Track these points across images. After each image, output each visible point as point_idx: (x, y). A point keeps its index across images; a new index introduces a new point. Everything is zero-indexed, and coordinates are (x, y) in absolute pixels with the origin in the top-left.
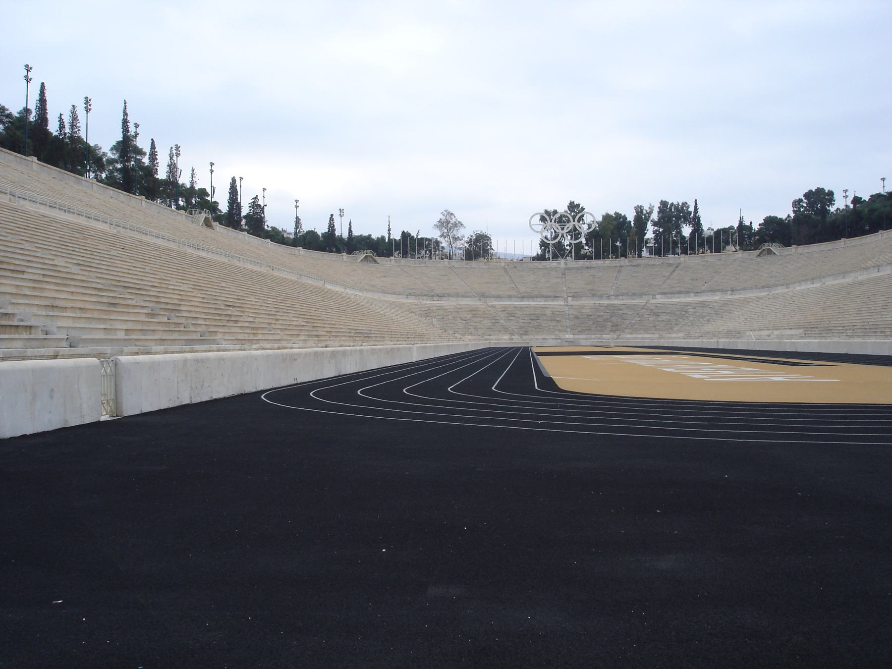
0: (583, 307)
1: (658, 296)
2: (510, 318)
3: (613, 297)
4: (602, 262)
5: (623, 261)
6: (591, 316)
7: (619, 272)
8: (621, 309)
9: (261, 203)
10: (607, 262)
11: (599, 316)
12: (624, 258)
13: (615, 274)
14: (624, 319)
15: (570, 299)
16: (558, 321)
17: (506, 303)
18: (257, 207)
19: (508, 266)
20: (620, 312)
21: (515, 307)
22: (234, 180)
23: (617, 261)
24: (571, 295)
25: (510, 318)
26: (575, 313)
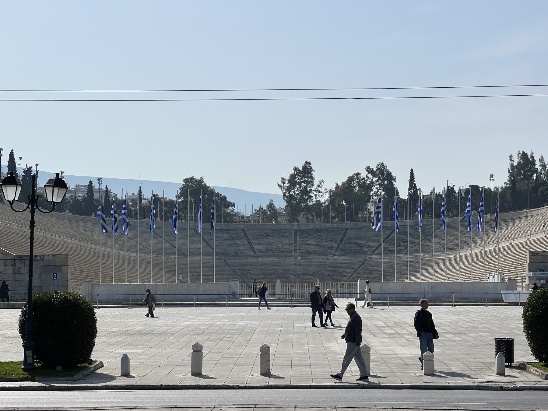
1: (374, 256)
2: (246, 274)
3: (337, 257)
4: (331, 225)
6: (316, 273)
7: (345, 234)
8: (342, 268)
9: (33, 174)
11: (323, 273)
12: (349, 222)
14: (345, 276)
15: (299, 258)
16: (287, 278)
19: (247, 227)
20: (341, 270)
22: (12, 154)
23: (343, 225)
24: (301, 254)
25: (246, 274)
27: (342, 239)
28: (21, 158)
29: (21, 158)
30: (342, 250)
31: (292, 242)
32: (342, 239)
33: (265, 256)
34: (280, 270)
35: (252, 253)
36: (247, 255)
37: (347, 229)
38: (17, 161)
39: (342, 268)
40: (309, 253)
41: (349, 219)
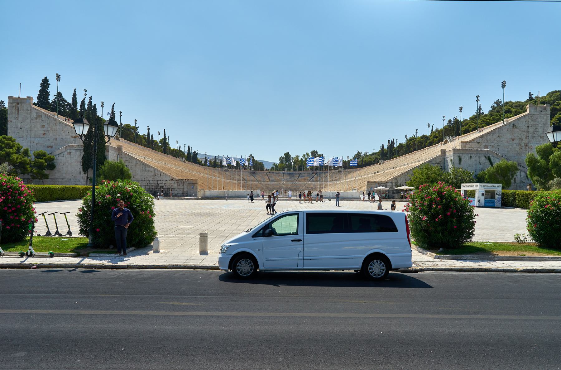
0: (288, 185)
1: (309, 183)
5: (301, 172)
7: (300, 175)
10: (297, 172)
13: (298, 176)
15: (285, 183)
17: (266, 183)
18: (195, 154)
21: (269, 185)
22: (189, 147)
26: (286, 187)
27: (299, 177)
28: (192, 148)
29: (192, 148)
30: (298, 180)
31: (282, 177)
32: (299, 177)
33: (273, 182)
34: (278, 186)
35: (269, 181)
36: (267, 182)
37: (300, 174)
38: (190, 149)
39: (298, 186)
40: (288, 181)
41: (301, 170)
